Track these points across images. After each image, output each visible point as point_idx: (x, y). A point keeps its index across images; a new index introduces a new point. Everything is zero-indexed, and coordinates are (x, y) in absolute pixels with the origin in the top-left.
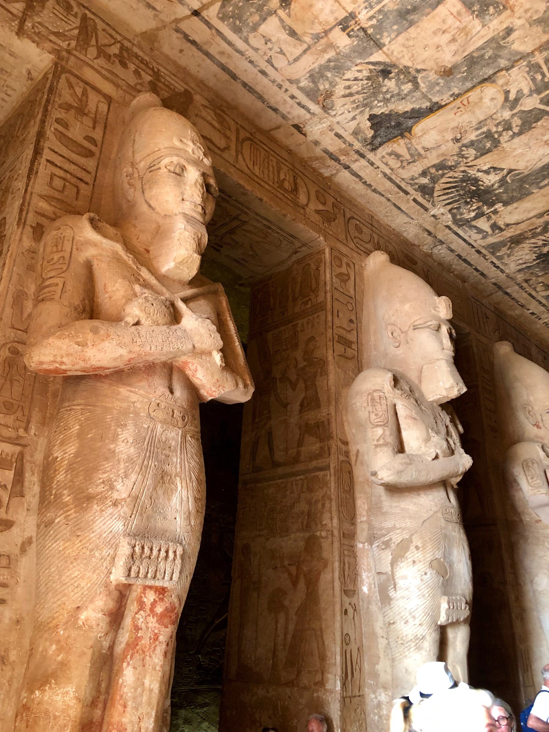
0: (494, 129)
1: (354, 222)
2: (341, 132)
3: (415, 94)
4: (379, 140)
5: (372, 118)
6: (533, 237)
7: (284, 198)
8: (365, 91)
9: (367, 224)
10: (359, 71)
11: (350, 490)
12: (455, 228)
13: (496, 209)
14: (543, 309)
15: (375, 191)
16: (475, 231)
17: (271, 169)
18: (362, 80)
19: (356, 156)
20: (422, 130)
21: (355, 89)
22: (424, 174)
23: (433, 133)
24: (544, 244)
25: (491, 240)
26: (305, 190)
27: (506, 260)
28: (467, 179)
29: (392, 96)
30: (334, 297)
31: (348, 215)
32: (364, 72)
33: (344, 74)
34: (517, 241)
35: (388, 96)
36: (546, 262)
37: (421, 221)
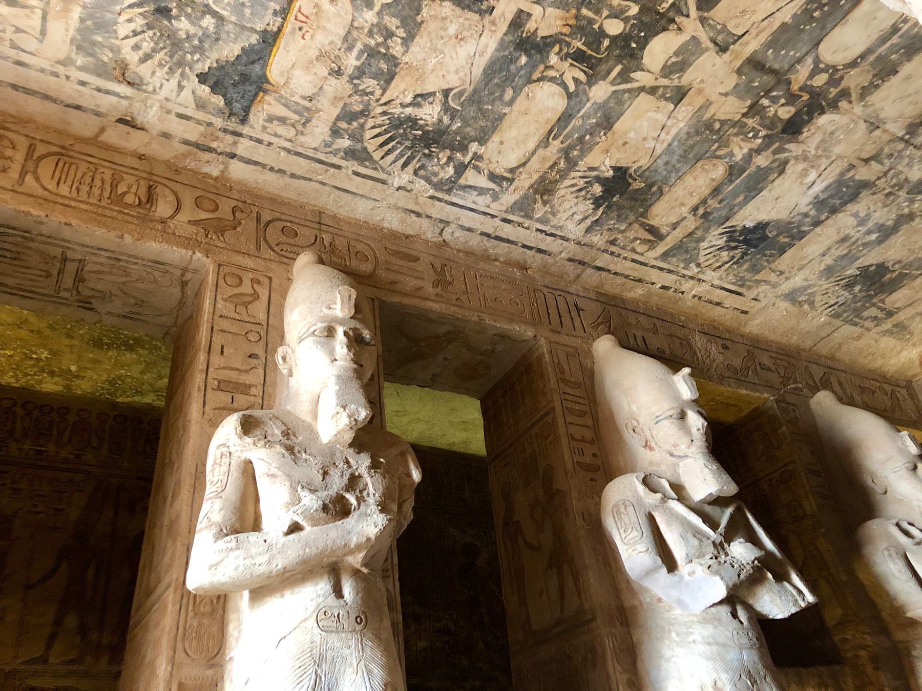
0: (372, 43)
1: (280, 225)
2: (182, 110)
3: (226, 28)
4: (237, 106)
5: (203, 78)
6: (563, 177)
7: (120, 216)
8: (161, 45)
9: (307, 223)
10: (130, 21)
11: (213, 611)
12: (446, 197)
13: (475, 154)
14: (673, 277)
15: (293, 176)
16: (476, 193)
17: (98, 183)
18: (144, 32)
19: (229, 138)
20: (282, 74)
21: (147, 46)
22: (336, 132)
23: (297, 72)
24: (586, 183)
25: (510, 198)
26: (171, 198)
27: (554, 221)
28: (397, 122)
29: (201, 41)
30: (216, 328)
31: (266, 216)
32: (138, 20)
33: (115, 32)
34: (544, 189)
35: (196, 42)
36: (614, 208)
37: (392, 201)
